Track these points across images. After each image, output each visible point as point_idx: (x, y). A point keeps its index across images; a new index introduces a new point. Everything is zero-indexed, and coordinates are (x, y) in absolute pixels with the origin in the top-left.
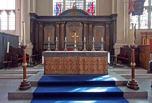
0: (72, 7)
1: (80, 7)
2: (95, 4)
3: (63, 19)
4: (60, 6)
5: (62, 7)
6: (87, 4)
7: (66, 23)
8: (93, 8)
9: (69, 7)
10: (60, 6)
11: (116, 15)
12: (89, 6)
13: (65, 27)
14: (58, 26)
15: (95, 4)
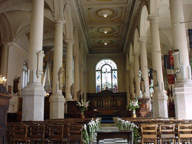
0: (105, 87)
1: (110, 87)
2: (117, 86)
3: (101, 95)
4: (99, 87)
5: (100, 87)
6: (113, 86)
7: (103, 96)
8: (116, 87)
9: (104, 87)
10: (99, 87)
11: (126, 93)
12: (114, 87)
13: (102, 98)
14: (99, 98)
15: (117, 86)
